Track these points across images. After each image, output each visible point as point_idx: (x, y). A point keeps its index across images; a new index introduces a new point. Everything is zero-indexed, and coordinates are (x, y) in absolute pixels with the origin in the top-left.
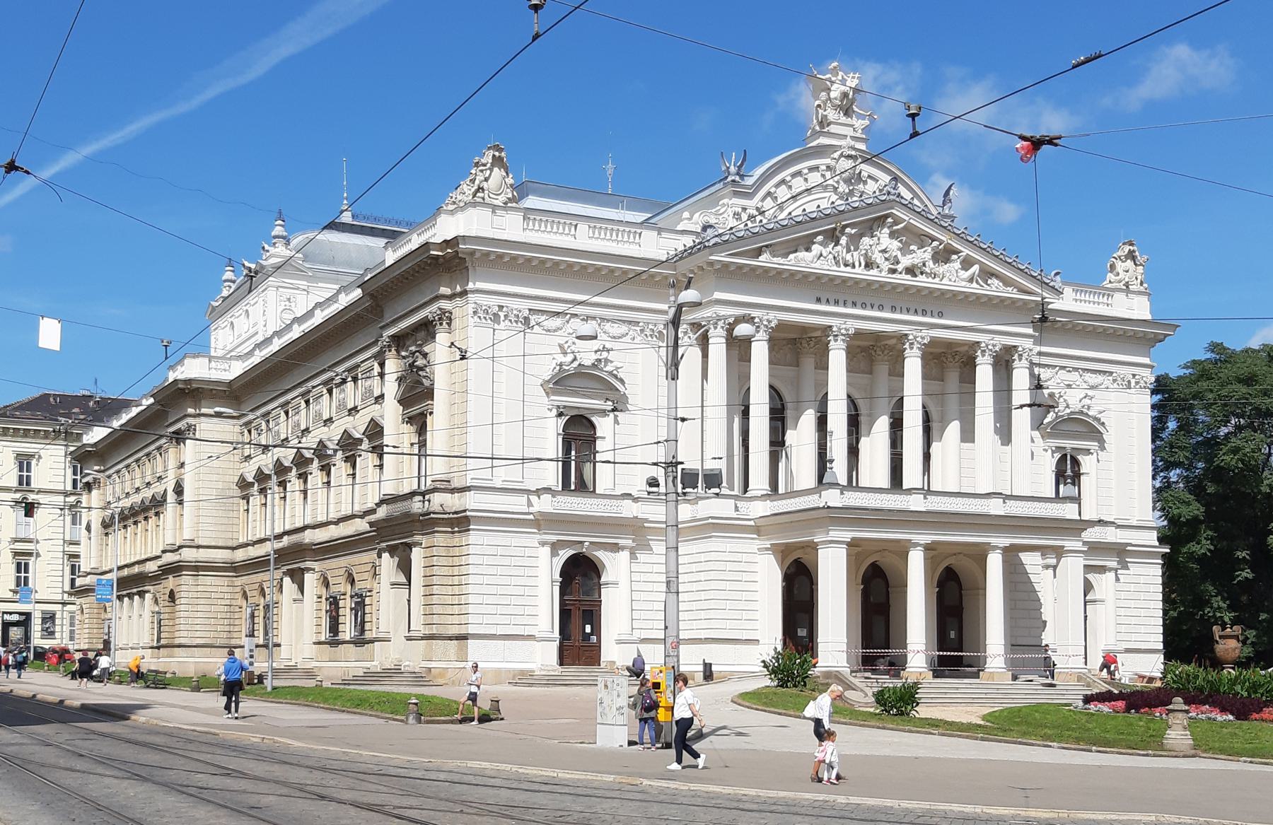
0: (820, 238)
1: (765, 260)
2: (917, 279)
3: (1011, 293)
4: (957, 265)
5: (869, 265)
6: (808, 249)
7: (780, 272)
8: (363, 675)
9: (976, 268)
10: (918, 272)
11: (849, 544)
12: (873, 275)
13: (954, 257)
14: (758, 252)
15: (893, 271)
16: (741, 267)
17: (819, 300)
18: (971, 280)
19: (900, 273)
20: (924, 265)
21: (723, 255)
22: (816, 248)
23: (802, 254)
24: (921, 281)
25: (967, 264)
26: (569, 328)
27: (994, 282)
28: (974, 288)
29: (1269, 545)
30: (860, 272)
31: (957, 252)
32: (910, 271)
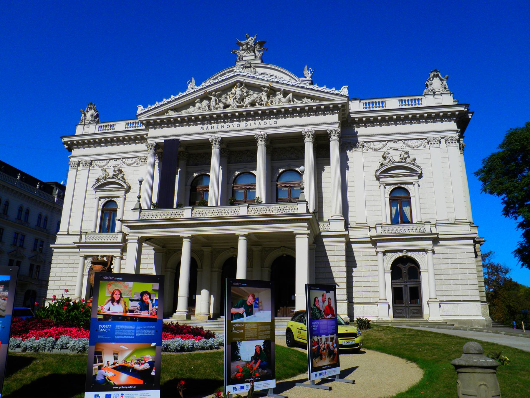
0: (197, 100)
1: (172, 114)
2: (255, 107)
3: (318, 103)
4: (282, 96)
5: (226, 106)
6: (194, 106)
7: (176, 119)
8: (300, 328)
9: (290, 95)
10: (257, 104)
11: (138, 240)
12: (228, 110)
13: (279, 93)
14: (166, 111)
15: (243, 106)
16: (155, 121)
17: (202, 128)
18: (289, 101)
19: (246, 106)
20: (262, 101)
21: (145, 117)
22: (197, 105)
23: (192, 109)
24: (258, 107)
25: (285, 93)
26: (109, 164)
27: (305, 100)
28: (292, 105)
29: (521, 225)
30: (220, 111)
31: (279, 90)
32: (253, 104)
